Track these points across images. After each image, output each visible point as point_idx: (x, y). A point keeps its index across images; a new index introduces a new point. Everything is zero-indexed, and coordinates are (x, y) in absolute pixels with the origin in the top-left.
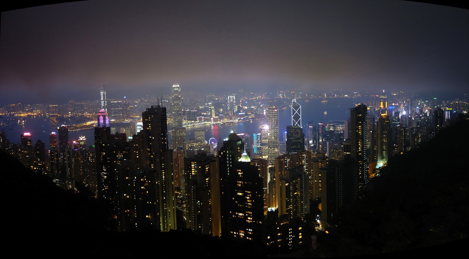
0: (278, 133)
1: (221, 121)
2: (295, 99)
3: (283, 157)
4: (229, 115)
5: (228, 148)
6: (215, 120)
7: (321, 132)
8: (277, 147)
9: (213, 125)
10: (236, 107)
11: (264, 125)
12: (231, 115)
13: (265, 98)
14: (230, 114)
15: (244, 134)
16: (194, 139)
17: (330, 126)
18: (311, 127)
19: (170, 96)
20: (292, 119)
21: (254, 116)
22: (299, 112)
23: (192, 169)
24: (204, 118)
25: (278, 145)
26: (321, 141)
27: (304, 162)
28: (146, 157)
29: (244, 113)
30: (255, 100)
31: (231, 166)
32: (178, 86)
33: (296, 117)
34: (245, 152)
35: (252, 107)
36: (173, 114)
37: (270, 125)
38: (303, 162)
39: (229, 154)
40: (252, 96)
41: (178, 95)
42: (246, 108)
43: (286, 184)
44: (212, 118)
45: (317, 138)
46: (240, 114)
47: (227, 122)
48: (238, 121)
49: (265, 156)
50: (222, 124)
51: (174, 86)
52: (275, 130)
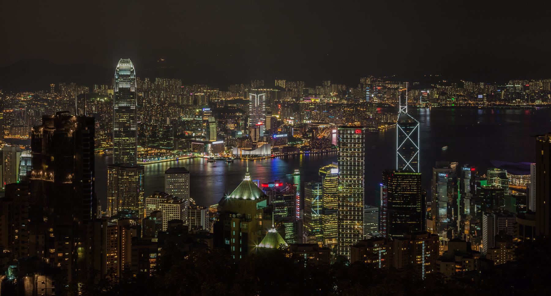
0: (362, 187)
1: (229, 152)
2: (406, 107)
3: (370, 242)
4: (251, 139)
6: (216, 149)
7: (468, 189)
8: (358, 220)
9: (211, 160)
11: (330, 165)
12: (255, 136)
13: (336, 101)
14: (253, 138)
16: (163, 194)
17: (493, 175)
18: (445, 175)
19: (109, 89)
21: (309, 142)
22: (414, 137)
23: (152, 265)
25: (362, 213)
26: (467, 210)
29: (286, 135)
30: (312, 105)
33: (408, 150)
36: (116, 131)
37: (343, 165)
40: (307, 95)
41: (128, 86)
42: (291, 122)
44: (210, 145)
45: (458, 204)
47: (244, 156)
48: (269, 152)
49: (330, 239)
50: (233, 158)
52: (356, 177)
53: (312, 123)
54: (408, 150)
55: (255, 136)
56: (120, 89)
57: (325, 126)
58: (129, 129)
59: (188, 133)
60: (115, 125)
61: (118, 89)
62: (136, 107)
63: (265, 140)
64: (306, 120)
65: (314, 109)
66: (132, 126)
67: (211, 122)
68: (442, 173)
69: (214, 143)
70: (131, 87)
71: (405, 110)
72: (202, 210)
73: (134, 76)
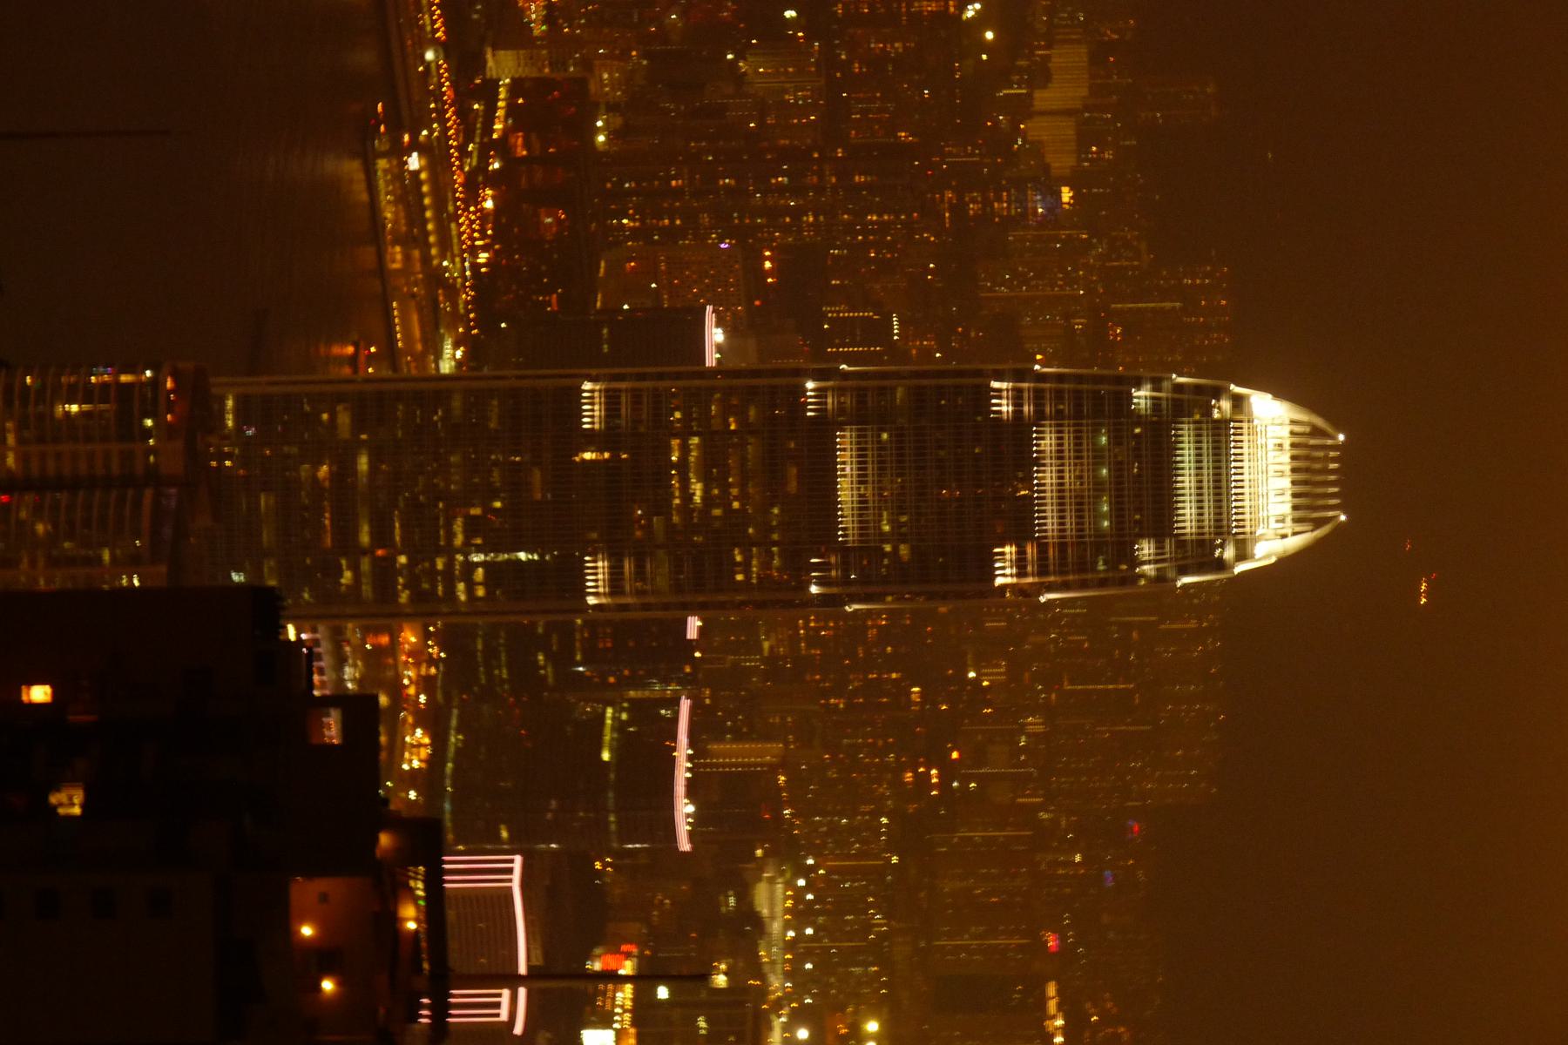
41: (1049, 522)
56: (1019, 431)
58: (594, 535)
60: (636, 396)
61: (1018, 413)
66: (628, 566)
70: (1042, 548)
73: (1160, 578)
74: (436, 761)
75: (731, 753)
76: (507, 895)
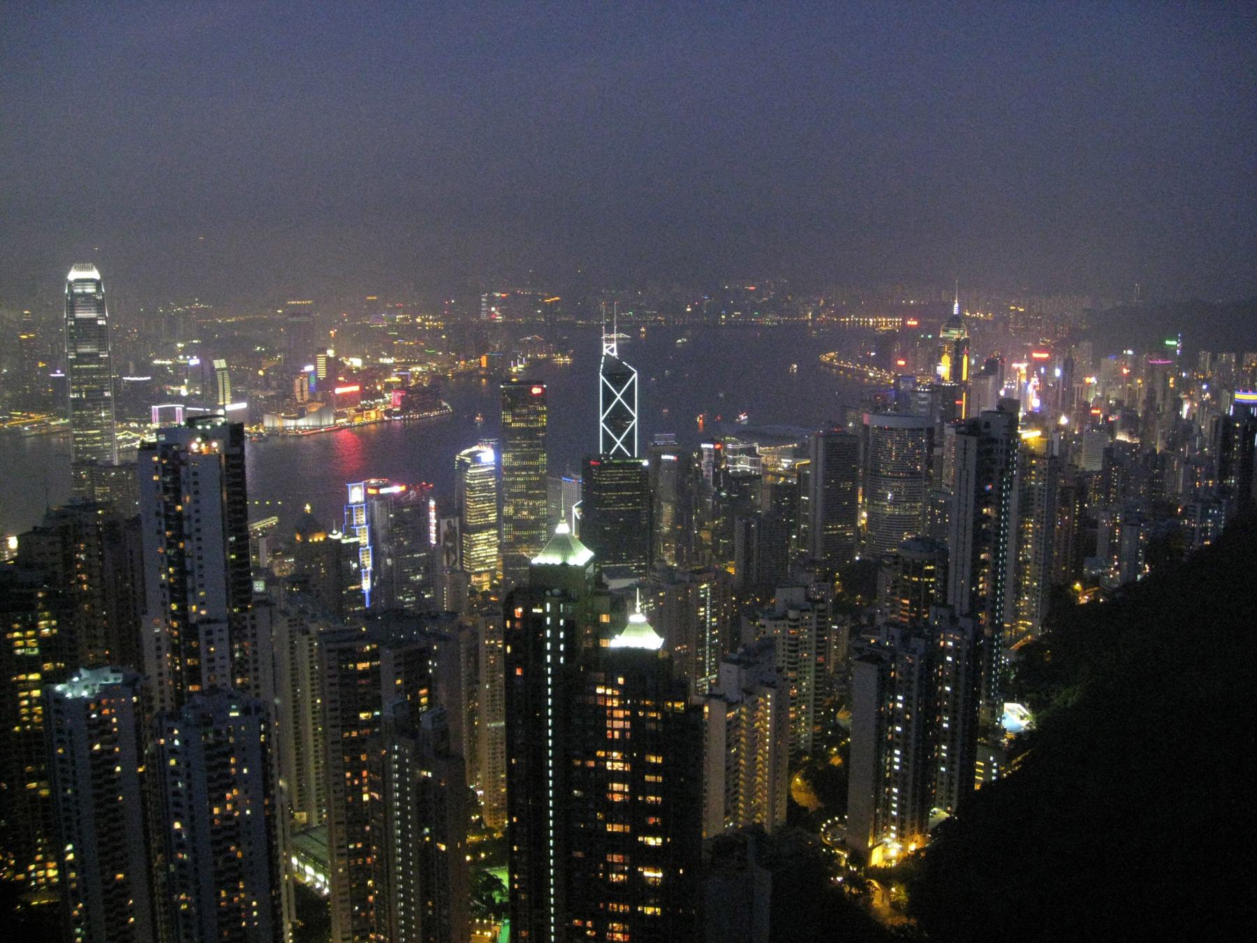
5: (552, 595)
10: (321, 361)
11: (475, 449)
15: (403, 488)
18: (672, 458)
20: (602, 424)
22: (628, 396)
24: (184, 409)
27: (705, 611)
28: (312, 656)
29: (356, 388)
31: (562, 660)
32: (95, 274)
33: (618, 419)
34: (638, 609)
35: (381, 360)
36: (73, 400)
38: (701, 614)
39: (556, 615)
40: (374, 308)
41: (93, 315)
43: (728, 715)
46: (338, 391)
48: (332, 422)
51: (73, 275)
53: (395, 363)
54: (618, 419)
55: (302, 391)
57: (419, 369)
59: (172, 391)
62: (109, 354)
63: (319, 399)
64: (383, 357)
65: (396, 338)
67: (218, 370)
68: (664, 454)
69: (231, 407)
71: (612, 350)
72: (260, 539)
74: (136, 422)
75: (132, 370)
76: (160, 409)
